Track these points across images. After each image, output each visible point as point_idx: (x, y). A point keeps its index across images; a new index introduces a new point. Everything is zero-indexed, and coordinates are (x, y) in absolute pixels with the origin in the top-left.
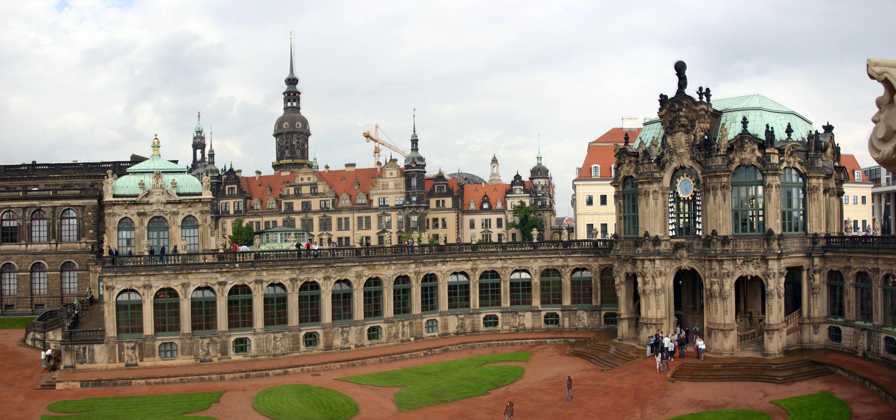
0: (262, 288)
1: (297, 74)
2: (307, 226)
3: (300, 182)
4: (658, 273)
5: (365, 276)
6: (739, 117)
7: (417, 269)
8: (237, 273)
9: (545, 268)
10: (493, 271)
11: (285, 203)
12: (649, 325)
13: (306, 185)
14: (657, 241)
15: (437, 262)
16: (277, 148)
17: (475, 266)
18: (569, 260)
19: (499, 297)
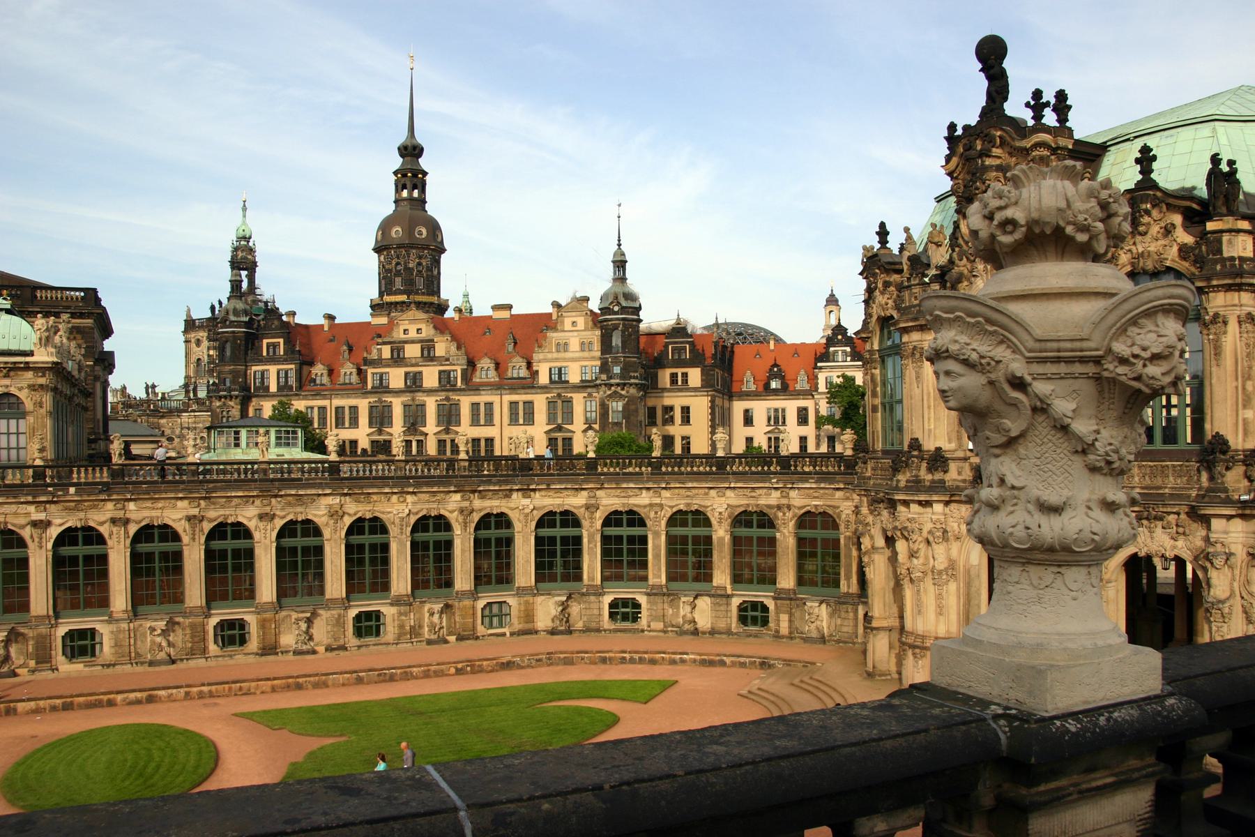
0: (126, 532)
1: (420, 139)
2: (414, 420)
3: (402, 336)
4: (939, 534)
5: (349, 515)
6: (1134, 150)
7: (466, 504)
8: (73, 504)
9: (742, 509)
10: (631, 512)
11: (373, 374)
12: (917, 651)
13: (413, 342)
14: (938, 460)
15: (511, 490)
16: (379, 274)
17: (593, 502)
18: (793, 494)
19: (644, 565)
